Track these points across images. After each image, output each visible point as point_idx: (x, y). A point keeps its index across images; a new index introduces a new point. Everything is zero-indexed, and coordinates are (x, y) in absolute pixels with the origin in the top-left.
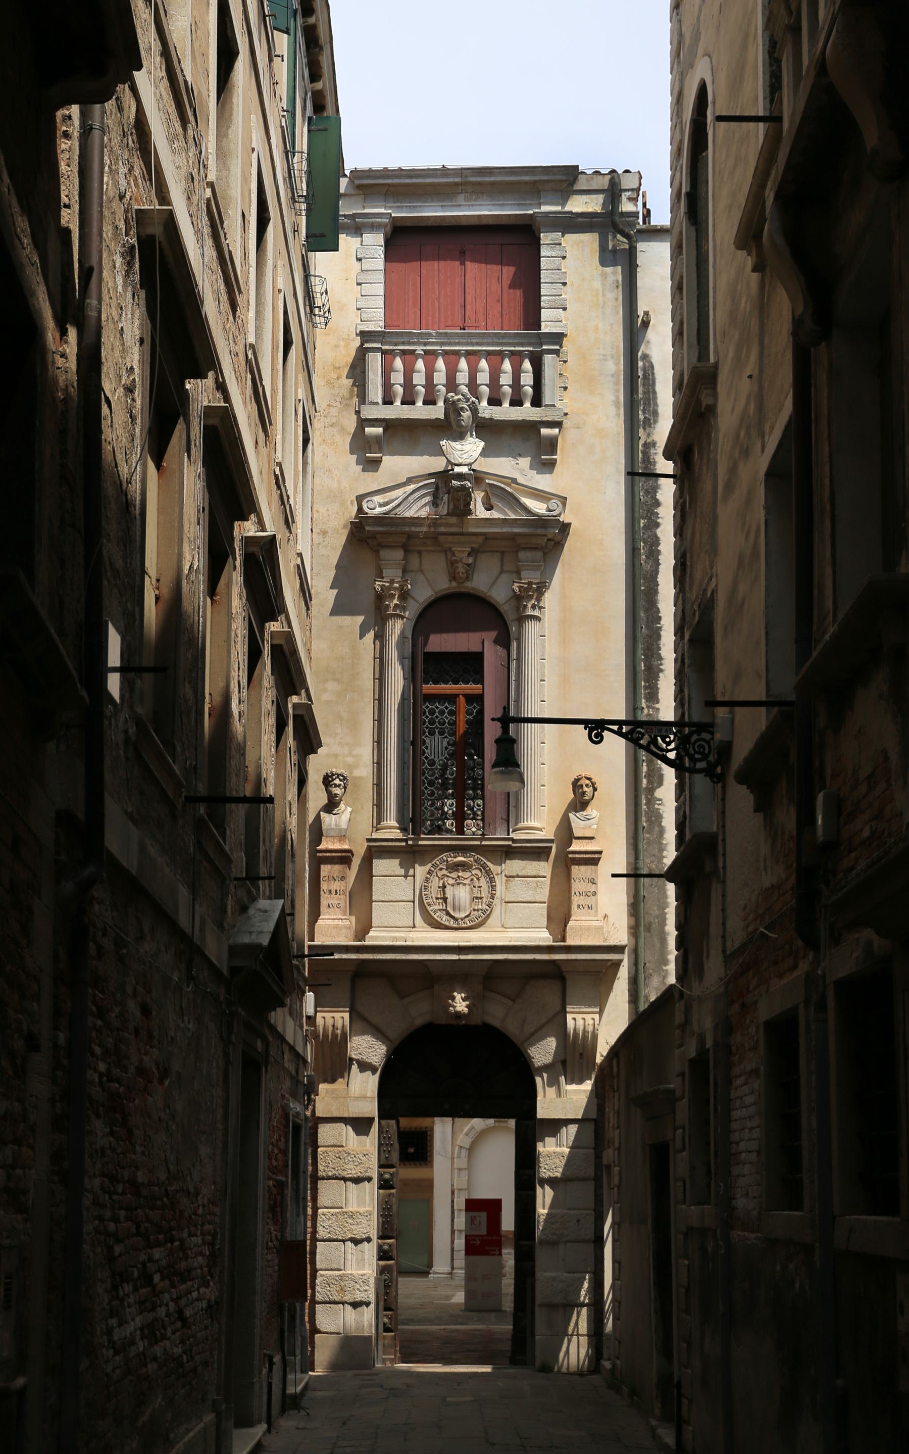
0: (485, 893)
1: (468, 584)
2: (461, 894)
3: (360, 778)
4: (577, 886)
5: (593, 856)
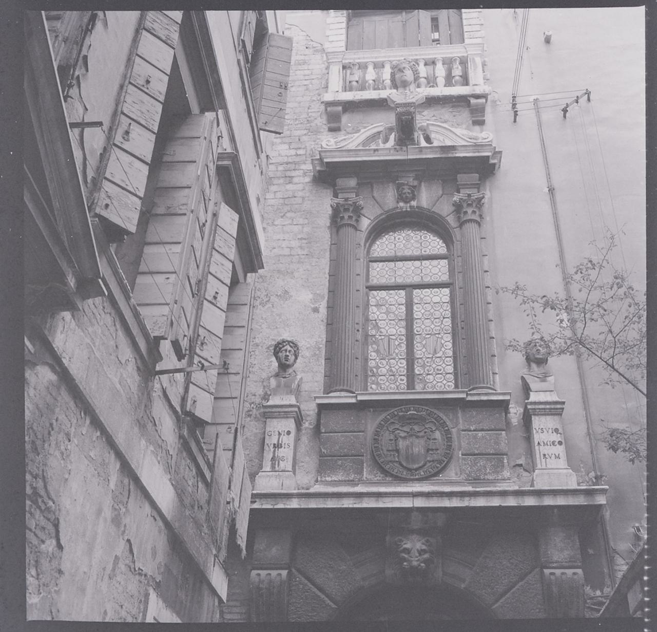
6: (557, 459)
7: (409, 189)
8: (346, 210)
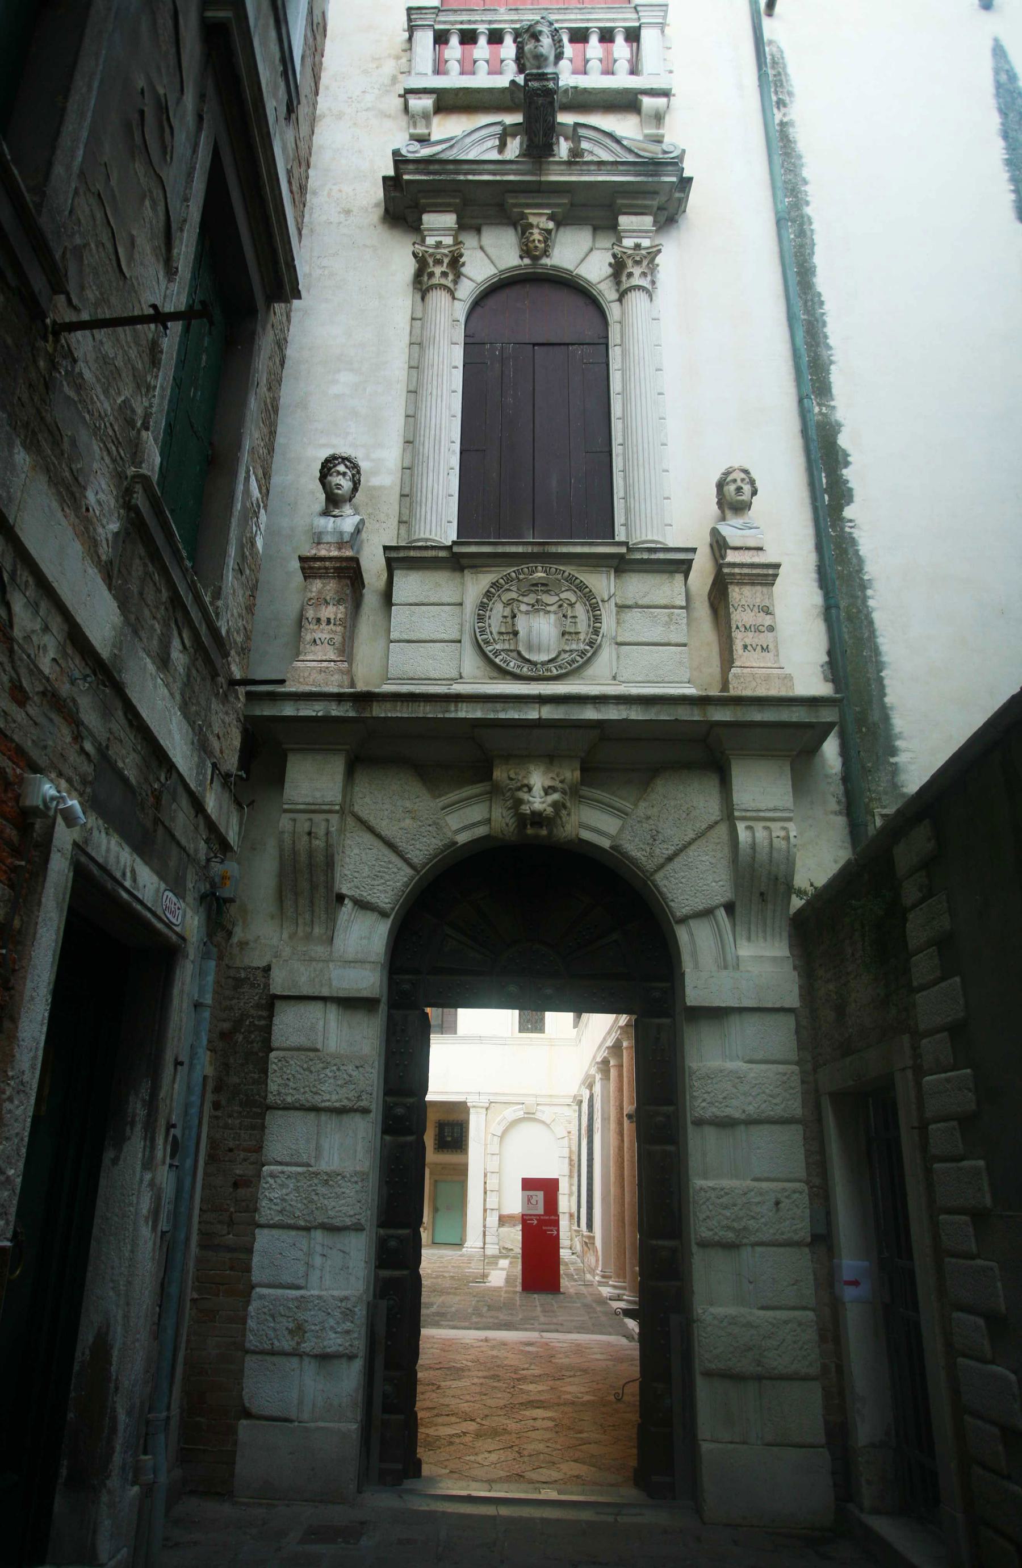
0: (583, 625)
1: (545, 261)
2: (541, 630)
3: (381, 488)
4: (739, 617)
5: (765, 571)
6: (764, 654)
7: (540, 234)
8: (438, 262)
